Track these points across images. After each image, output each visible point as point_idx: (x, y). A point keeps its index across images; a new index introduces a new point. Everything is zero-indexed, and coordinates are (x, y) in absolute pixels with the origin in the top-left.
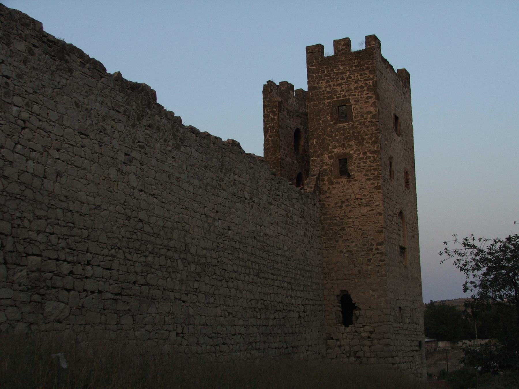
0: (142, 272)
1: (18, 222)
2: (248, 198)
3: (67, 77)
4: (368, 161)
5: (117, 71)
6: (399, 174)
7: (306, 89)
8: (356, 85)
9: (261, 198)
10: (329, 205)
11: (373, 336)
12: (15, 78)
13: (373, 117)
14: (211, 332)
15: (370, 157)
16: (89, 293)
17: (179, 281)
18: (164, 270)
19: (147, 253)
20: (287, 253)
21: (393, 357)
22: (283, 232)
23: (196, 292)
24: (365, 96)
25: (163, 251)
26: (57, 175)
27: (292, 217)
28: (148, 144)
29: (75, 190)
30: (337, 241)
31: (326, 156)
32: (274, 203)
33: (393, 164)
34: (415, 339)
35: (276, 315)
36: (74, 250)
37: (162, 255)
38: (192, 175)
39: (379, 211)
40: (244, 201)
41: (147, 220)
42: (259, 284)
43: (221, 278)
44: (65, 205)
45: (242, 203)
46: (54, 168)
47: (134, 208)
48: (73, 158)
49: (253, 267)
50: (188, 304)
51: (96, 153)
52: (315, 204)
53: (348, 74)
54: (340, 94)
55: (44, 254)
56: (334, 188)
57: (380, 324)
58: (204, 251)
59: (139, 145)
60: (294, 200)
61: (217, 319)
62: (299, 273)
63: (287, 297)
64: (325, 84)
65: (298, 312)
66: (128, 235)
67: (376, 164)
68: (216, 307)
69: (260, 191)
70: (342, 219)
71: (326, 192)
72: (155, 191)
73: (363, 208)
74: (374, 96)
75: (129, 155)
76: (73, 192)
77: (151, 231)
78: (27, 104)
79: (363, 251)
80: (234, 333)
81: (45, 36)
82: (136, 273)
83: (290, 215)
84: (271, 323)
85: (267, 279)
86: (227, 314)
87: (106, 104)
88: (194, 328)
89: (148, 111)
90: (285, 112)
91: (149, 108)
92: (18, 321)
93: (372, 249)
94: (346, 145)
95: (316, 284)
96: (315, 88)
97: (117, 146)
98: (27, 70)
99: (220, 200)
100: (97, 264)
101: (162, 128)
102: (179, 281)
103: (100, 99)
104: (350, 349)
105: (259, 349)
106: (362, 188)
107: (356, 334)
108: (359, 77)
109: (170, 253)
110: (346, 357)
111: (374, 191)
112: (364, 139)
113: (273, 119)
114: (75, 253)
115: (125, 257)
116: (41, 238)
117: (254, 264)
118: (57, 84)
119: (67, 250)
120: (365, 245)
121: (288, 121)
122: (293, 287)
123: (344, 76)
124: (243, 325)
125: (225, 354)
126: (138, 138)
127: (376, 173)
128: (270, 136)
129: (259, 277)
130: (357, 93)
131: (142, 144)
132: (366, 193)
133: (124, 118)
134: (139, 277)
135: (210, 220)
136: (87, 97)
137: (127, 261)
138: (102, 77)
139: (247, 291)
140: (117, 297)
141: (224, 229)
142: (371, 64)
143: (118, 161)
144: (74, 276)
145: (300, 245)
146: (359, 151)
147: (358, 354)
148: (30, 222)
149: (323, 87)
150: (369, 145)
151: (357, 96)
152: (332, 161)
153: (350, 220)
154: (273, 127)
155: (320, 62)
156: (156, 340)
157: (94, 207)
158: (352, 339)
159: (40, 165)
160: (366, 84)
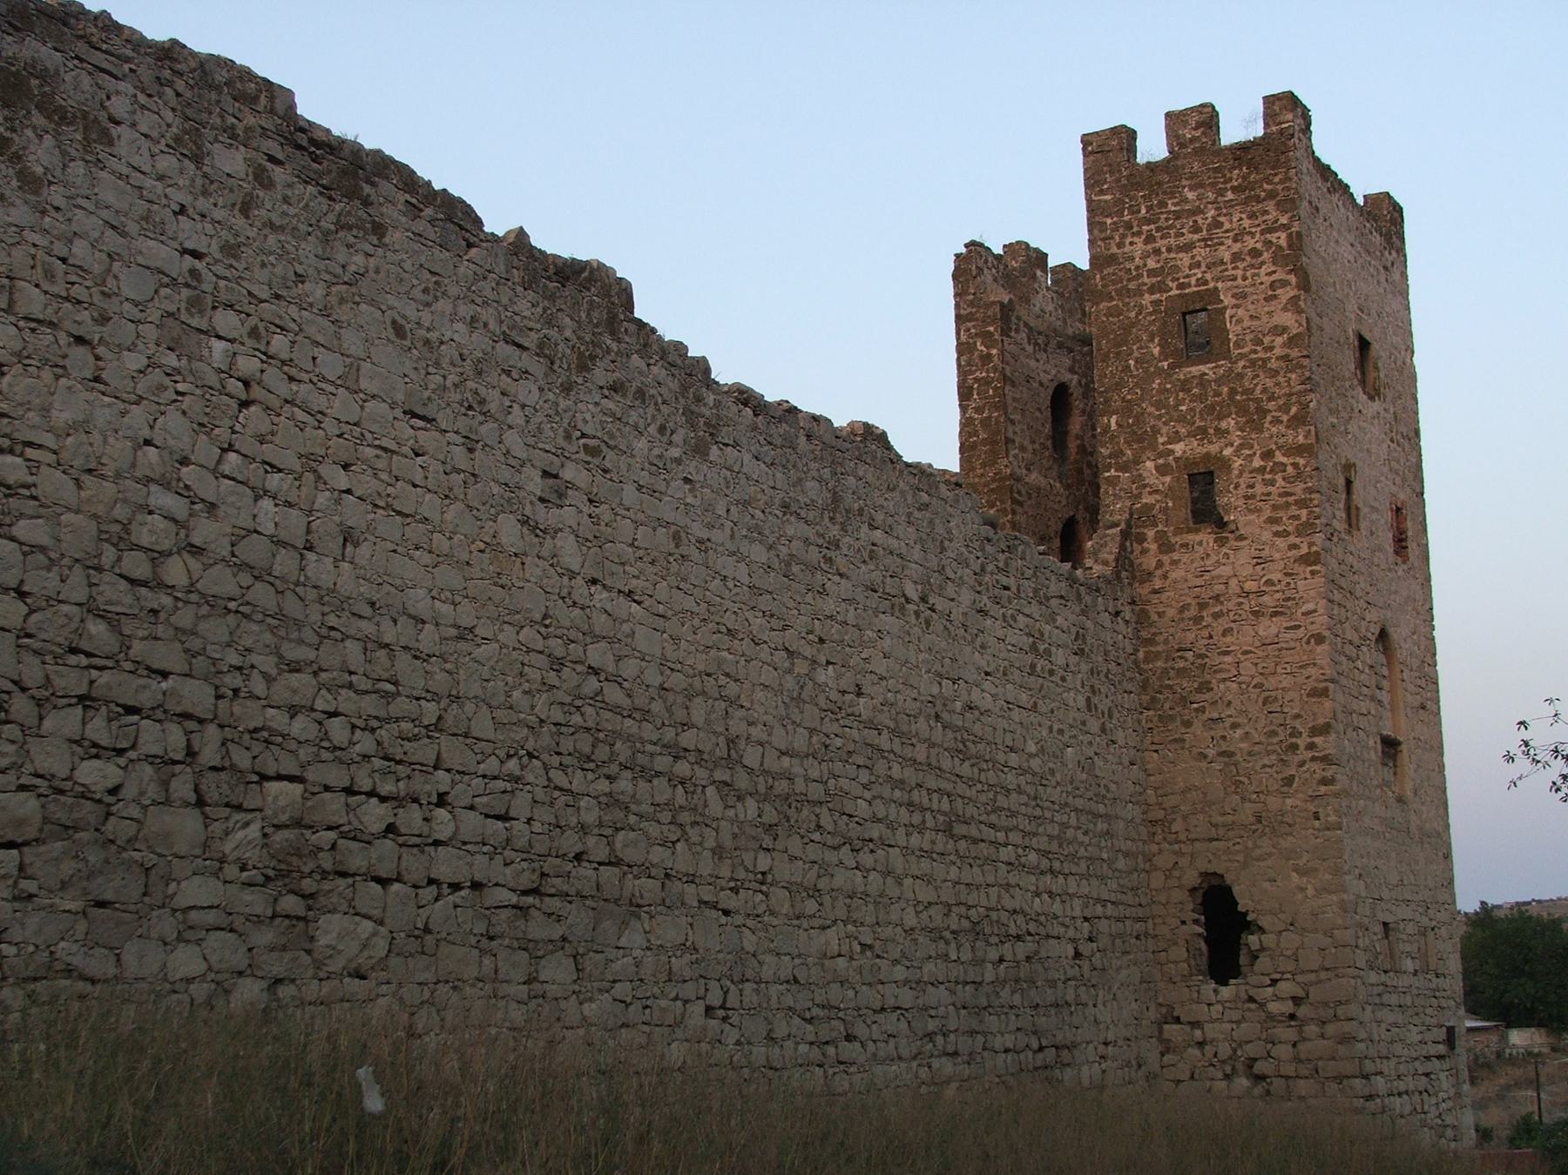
0: (600, 825)
1: (234, 680)
2: (916, 598)
3: (370, 249)
4: (1279, 477)
5: (515, 226)
6: (1375, 516)
7: (1084, 264)
8: (1237, 247)
10: (1160, 615)
11: (1302, 1011)
12: (218, 256)
13: (1292, 342)
16: (446, 891)
17: (713, 851)
18: (665, 817)
19: (614, 769)
20: (1035, 763)
21: (1366, 1077)
22: (1024, 698)
23: (762, 883)
24: (1265, 279)
25: (663, 763)
26: (345, 540)
27: (1048, 652)
28: (611, 443)
29: (398, 582)
30: (1187, 724)
31: (1149, 465)
33: (1357, 485)
36: (399, 762)
37: (658, 774)
39: (1315, 629)
40: (902, 608)
41: (611, 668)
43: (838, 840)
44: (367, 628)
45: (897, 613)
46: (336, 518)
47: (573, 634)
48: (390, 490)
49: (935, 807)
50: (738, 920)
51: (459, 471)
52: (1117, 614)
54: (1188, 276)
55: (310, 775)
56: (1174, 563)
57: (1323, 975)
58: (786, 761)
59: (585, 446)
60: (1054, 602)
62: (1073, 821)
63: (1038, 895)
64: (1140, 245)
65: (1073, 940)
66: (557, 714)
67: (1302, 486)
68: (824, 928)
69: (952, 576)
71: (1150, 574)
72: (635, 582)
73: (1265, 621)
74: (1292, 279)
75: (556, 476)
76: (393, 590)
78: (254, 333)
80: (877, 1006)
81: (302, 130)
82: (583, 829)
83: (1042, 648)
84: (989, 975)
85: (975, 841)
87: (485, 325)
88: (757, 991)
91: (613, 333)
92: (240, 973)
93: (1294, 747)
95: (1126, 855)
96: (1112, 259)
97: (520, 451)
98: (252, 233)
99: (829, 605)
100: (467, 801)
101: (652, 392)
102: (713, 851)
103: (465, 310)
104: (1235, 1051)
105: (956, 1054)
106: (1260, 561)
107: (1253, 1006)
108: (1246, 223)
109: (683, 768)
110: (1220, 1075)
111: (1298, 568)
112: (1263, 412)
114: (402, 770)
115: (549, 779)
116: (301, 727)
117: (935, 796)
118: (339, 271)
119: (378, 763)
120: (1274, 733)
121: (1033, 363)
122: (1057, 865)
123: (1199, 219)
124: (906, 982)
125: (852, 1069)
126: (580, 425)
127: (1304, 512)
128: (978, 410)
129: (952, 836)
131: (592, 442)
132: (1275, 577)
133: (537, 367)
134: (591, 841)
135: (801, 667)
136: (428, 305)
137: (556, 794)
138: (470, 245)
139: (915, 877)
140: (530, 900)
141: (844, 692)
143: (522, 494)
144: (401, 840)
147: (1259, 1067)
148: (269, 679)
149: (1137, 254)
151: (1239, 281)
152: (1168, 479)
153: (1228, 659)
154: (986, 382)
155: (1124, 181)
156: (646, 1028)
157: (453, 632)
158: (1238, 1022)
159: (294, 512)
160: (1268, 243)
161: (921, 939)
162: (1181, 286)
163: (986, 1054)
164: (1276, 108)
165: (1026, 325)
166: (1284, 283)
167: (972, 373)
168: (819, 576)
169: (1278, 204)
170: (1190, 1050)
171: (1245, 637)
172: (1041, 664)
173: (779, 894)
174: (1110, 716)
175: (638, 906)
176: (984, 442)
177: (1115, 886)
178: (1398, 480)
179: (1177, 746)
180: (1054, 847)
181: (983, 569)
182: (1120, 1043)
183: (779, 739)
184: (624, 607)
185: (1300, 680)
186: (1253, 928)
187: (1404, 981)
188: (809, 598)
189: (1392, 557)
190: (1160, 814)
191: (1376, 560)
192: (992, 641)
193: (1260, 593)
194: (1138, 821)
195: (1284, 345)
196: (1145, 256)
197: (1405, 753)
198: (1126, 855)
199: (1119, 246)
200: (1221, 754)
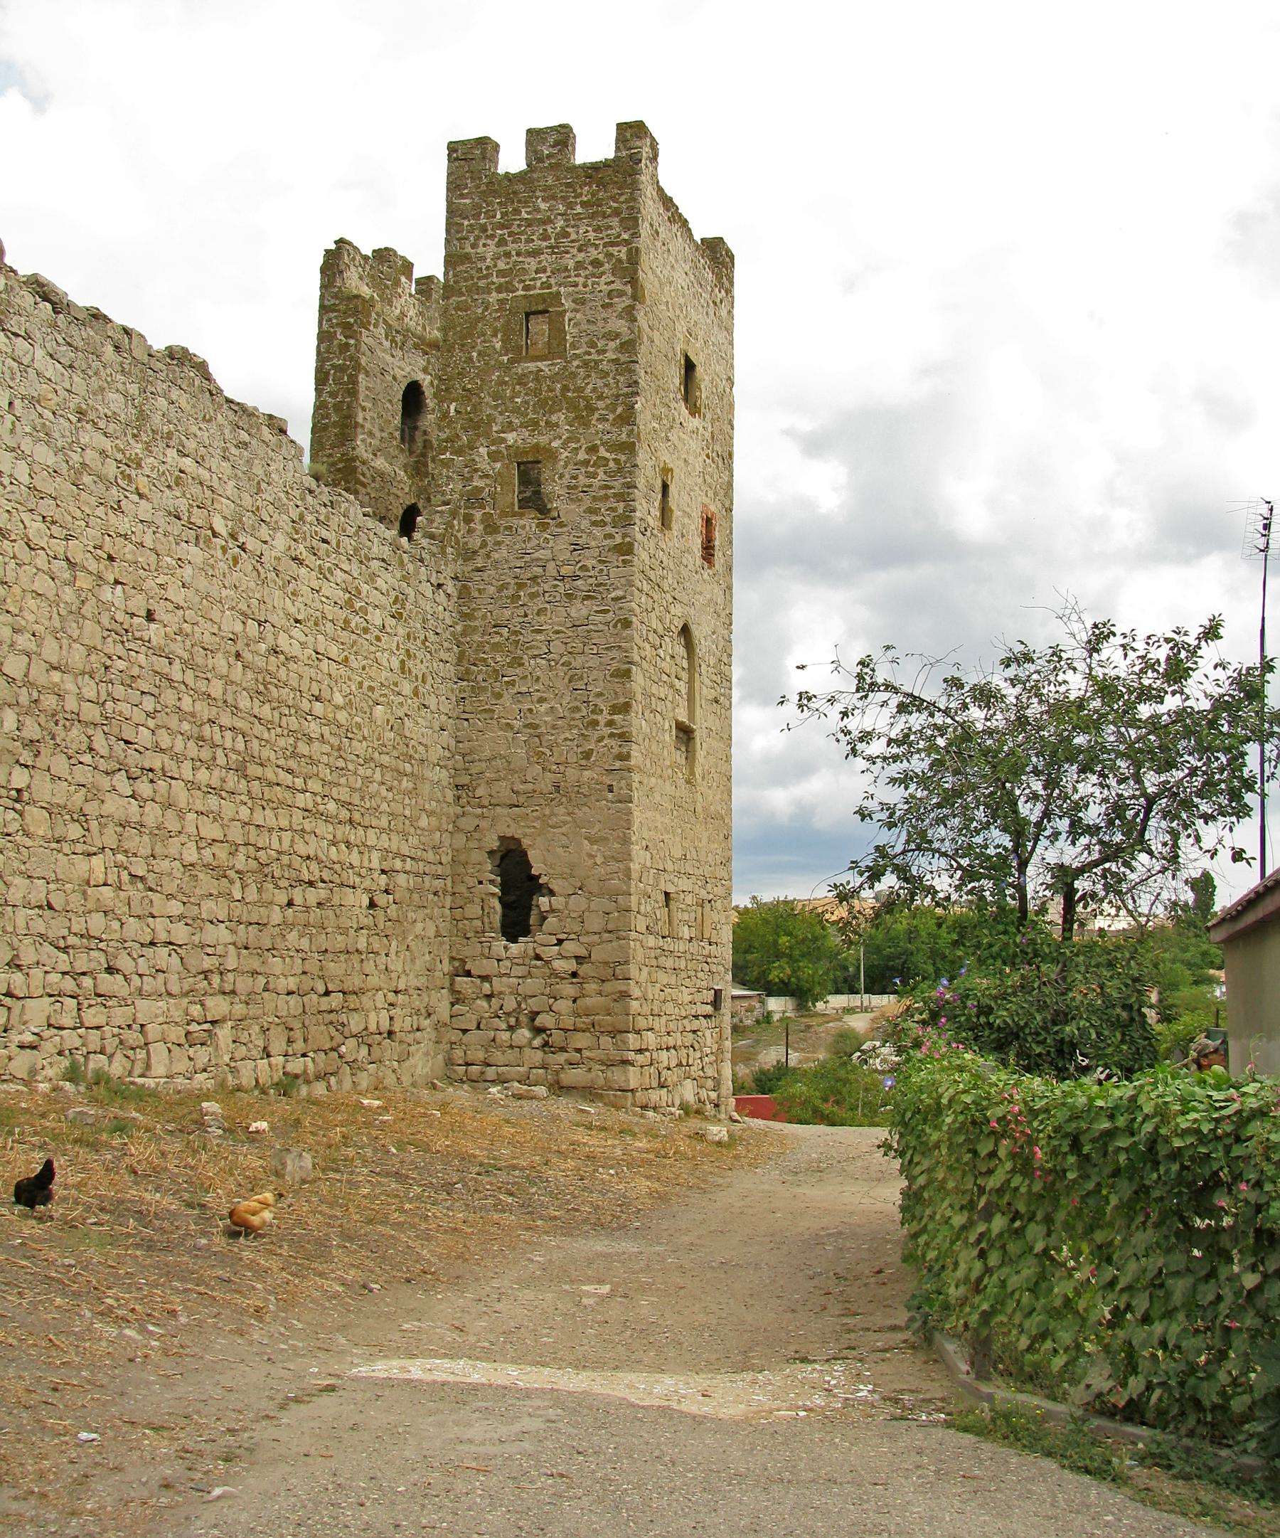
2: (224, 532)
4: (600, 471)
6: (686, 520)
8: (580, 257)
9: (268, 538)
11: (585, 969)
14: (66, 932)
20: (342, 716)
21: (638, 1032)
22: (334, 651)
23: (17, 801)
30: (498, 696)
31: (483, 450)
32: (310, 560)
33: (673, 489)
34: (704, 984)
38: (28, 429)
49: (228, 744)
52: (440, 586)
53: (560, 223)
54: (534, 279)
56: (498, 543)
58: (56, 676)
60: (375, 564)
61: (90, 891)
62: (378, 776)
70: (516, 633)
71: (475, 552)
74: (629, 289)
79: (570, 727)
80: (148, 939)
83: (358, 605)
84: (276, 917)
85: (270, 784)
86: (125, 876)
90: (381, 331)
93: (595, 723)
94: (543, 424)
95: (430, 814)
96: (467, 257)
99: (124, 524)
105: (233, 992)
106: (576, 547)
108: (592, 235)
110: (504, 1026)
111: (613, 557)
112: (591, 409)
113: (346, 347)
117: (228, 734)
120: (578, 709)
121: (388, 358)
122: (357, 816)
124: (181, 917)
128: (333, 395)
130: (581, 280)
132: (590, 563)
142: (626, 201)
145: (385, 695)
147: (539, 1021)
150: (607, 426)
151: (580, 287)
152: (498, 465)
154: (341, 369)
155: (483, 188)
161: (201, 876)
162: (526, 288)
164: (628, 135)
165: (385, 322)
166: (621, 294)
167: (329, 359)
168: (114, 491)
169: (621, 221)
170: (478, 1002)
171: (555, 619)
172: (356, 621)
173: (35, 815)
174: (424, 681)
176: (335, 424)
178: (710, 493)
179: (486, 716)
180: (356, 799)
181: (302, 517)
182: (411, 991)
183: (51, 651)
185: (606, 660)
186: (545, 891)
187: (682, 946)
188: (100, 511)
189: (699, 561)
190: (465, 780)
193: (576, 577)
196: (496, 258)
197: (698, 741)
199: (474, 246)
200: (526, 726)
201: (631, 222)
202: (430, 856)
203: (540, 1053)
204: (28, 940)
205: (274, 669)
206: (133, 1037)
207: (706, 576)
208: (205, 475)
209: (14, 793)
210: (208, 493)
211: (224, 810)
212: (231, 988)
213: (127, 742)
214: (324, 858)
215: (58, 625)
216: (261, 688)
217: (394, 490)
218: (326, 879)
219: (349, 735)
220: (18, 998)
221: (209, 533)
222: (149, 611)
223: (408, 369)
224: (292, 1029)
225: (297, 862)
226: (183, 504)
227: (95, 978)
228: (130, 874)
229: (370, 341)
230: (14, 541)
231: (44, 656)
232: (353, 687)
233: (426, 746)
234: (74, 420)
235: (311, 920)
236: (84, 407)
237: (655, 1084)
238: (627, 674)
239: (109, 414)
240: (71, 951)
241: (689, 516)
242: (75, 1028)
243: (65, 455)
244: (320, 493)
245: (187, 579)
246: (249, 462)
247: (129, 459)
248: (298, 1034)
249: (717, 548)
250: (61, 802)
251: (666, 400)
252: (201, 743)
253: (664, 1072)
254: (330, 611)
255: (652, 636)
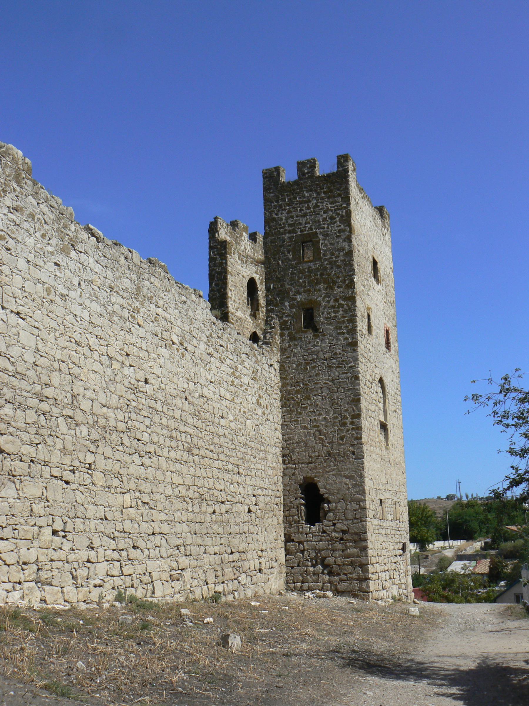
2: (178, 343)
6: (378, 331)
8: (325, 215)
9: (197, 345)
11: (347, 536)
15: (344, 305)
18: (33, 430)
20: (233, 425)
21: (372, 565)
22: (228, 396)
23: (89, 469)
28: (12, 235)
30: (300, 413)
32: (215, 354)
34: (398, 540)
35: (217, 508)
38: (88, 295)
40: (170, 346)
42: (192, 464)
49: (184, 440)
50: (74, 486)
52: (271, 365)
53: (314, 202)
58: (105, 410)
60: (243, 356)
61: (124, 510)
62: (249, 452)
65: (247, 504)
71: (286, 349)
72: (21, 307)
77: (11, 368)
80: (152, 532)
83: (237, 374)
84: (208, 519)
85: (203, 457)
86: (140, 503)
89: (15, 186)
90: (236, 256)
91: (18, 182)
96: (274, 219)
99: (132, 339)
101: (40, 216)
109: (45, 406)
112: (334, 282)
117: (183, 435)
120: (337, 418)
121: (240, 268)
122: (241, 471)
123: (310, 204)
124: (166, 521)
125: (136, 563)
130: (326, 226)
145: (251, 415)
146: (329, 297)
147: (326, 562)
150: (342, 289)
151: (326, 229)
152: (294, 310)
160: (338, 214)
161: (174, 501)
163: (205, 555)
164: (342, 160)
166: (344, 231)
168: (128, 323)
169: (342, 198)
172: (236, 381)
175: (14, 476)
177: (267, 481)
178: (387, 319)
181: (211, 335)
182: (268, 550)
183: (102, 398)
184: (13, 319)
187: (388, 523)
189: (385, 349)
191: (378, 348)
192: (214, 368)
194: (278, 454)
195: (344, 255)
196: (287, 219)
198: (273, 468)
200: (314, 427)
201: (347, 199)
202: (274, 487)
203: (328, 577)
204: (96, 535)
205: (202, 404)
206: (146, 579)
207: (388, 356)
208: (168, 316)
209: (87, 465)
210: (169, 324)
211: (183, 470)
212: (189, 553)
213: (138, 440)
214: (228, 491)
215: (105, 386)
216: (197, 413)
217: (246, 326)
218: (229, 500)
219: (237, 434)
220: (93, 563)
221: (171, 342)
222: (146, 379)
223: (249, 272)
224: (217, 571)
225: (216, 493)
226: (158, 330)
227: (128, 552)
228: (142, 502)
229: (232, 260)
230: (84, 347)
231: (99, 401)
232: (237, 412)
233: (269, 438)
234: (108, 291)
235: (224, 520)
236: (113, 285)
237: (381, 588)
238: (359, 400)
239: (124, 288)
240: (116, 539)
241: (379, 329)
242: (119, 576)
243: (105, 307)
244: (218, 324)
245: (162, 364)
246: (187, 310)
247: (134, 309)
248: (219, 573)
249: (391, 343)
250: (110, 469)
251: (366, 277)
252: (171, 439)
253: (384, 582)
254: (226, 378)
255: (368, 383)
